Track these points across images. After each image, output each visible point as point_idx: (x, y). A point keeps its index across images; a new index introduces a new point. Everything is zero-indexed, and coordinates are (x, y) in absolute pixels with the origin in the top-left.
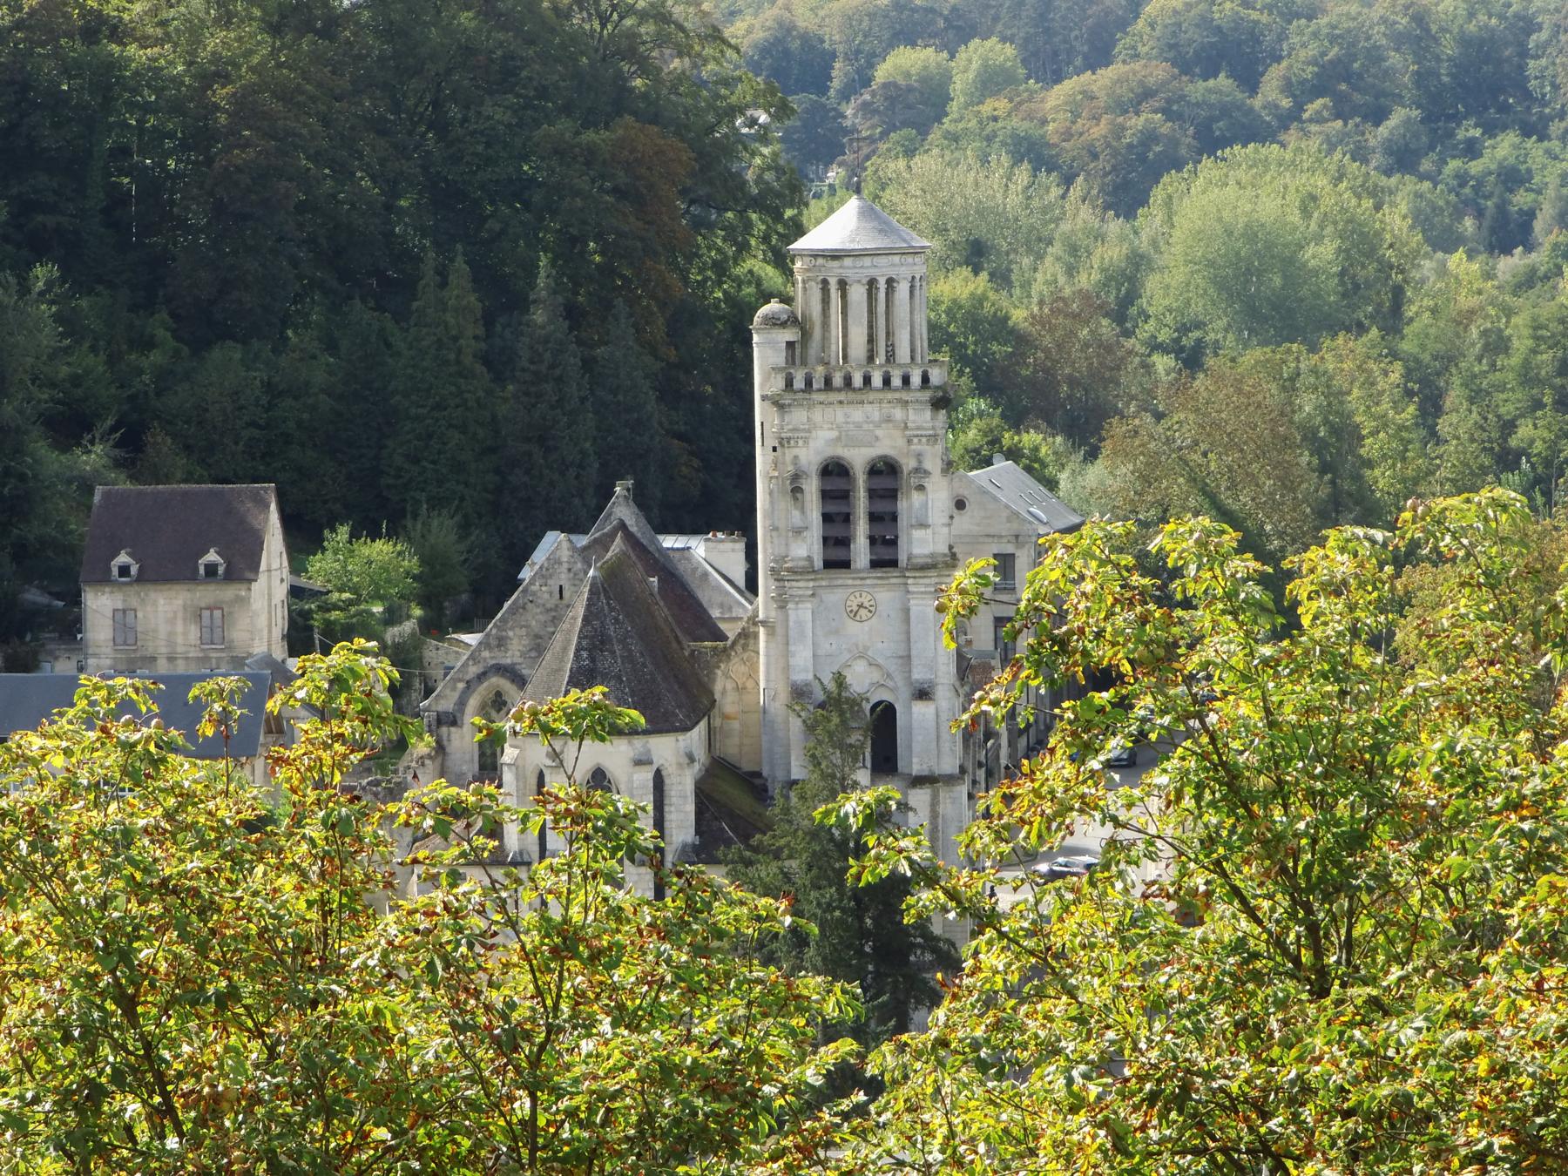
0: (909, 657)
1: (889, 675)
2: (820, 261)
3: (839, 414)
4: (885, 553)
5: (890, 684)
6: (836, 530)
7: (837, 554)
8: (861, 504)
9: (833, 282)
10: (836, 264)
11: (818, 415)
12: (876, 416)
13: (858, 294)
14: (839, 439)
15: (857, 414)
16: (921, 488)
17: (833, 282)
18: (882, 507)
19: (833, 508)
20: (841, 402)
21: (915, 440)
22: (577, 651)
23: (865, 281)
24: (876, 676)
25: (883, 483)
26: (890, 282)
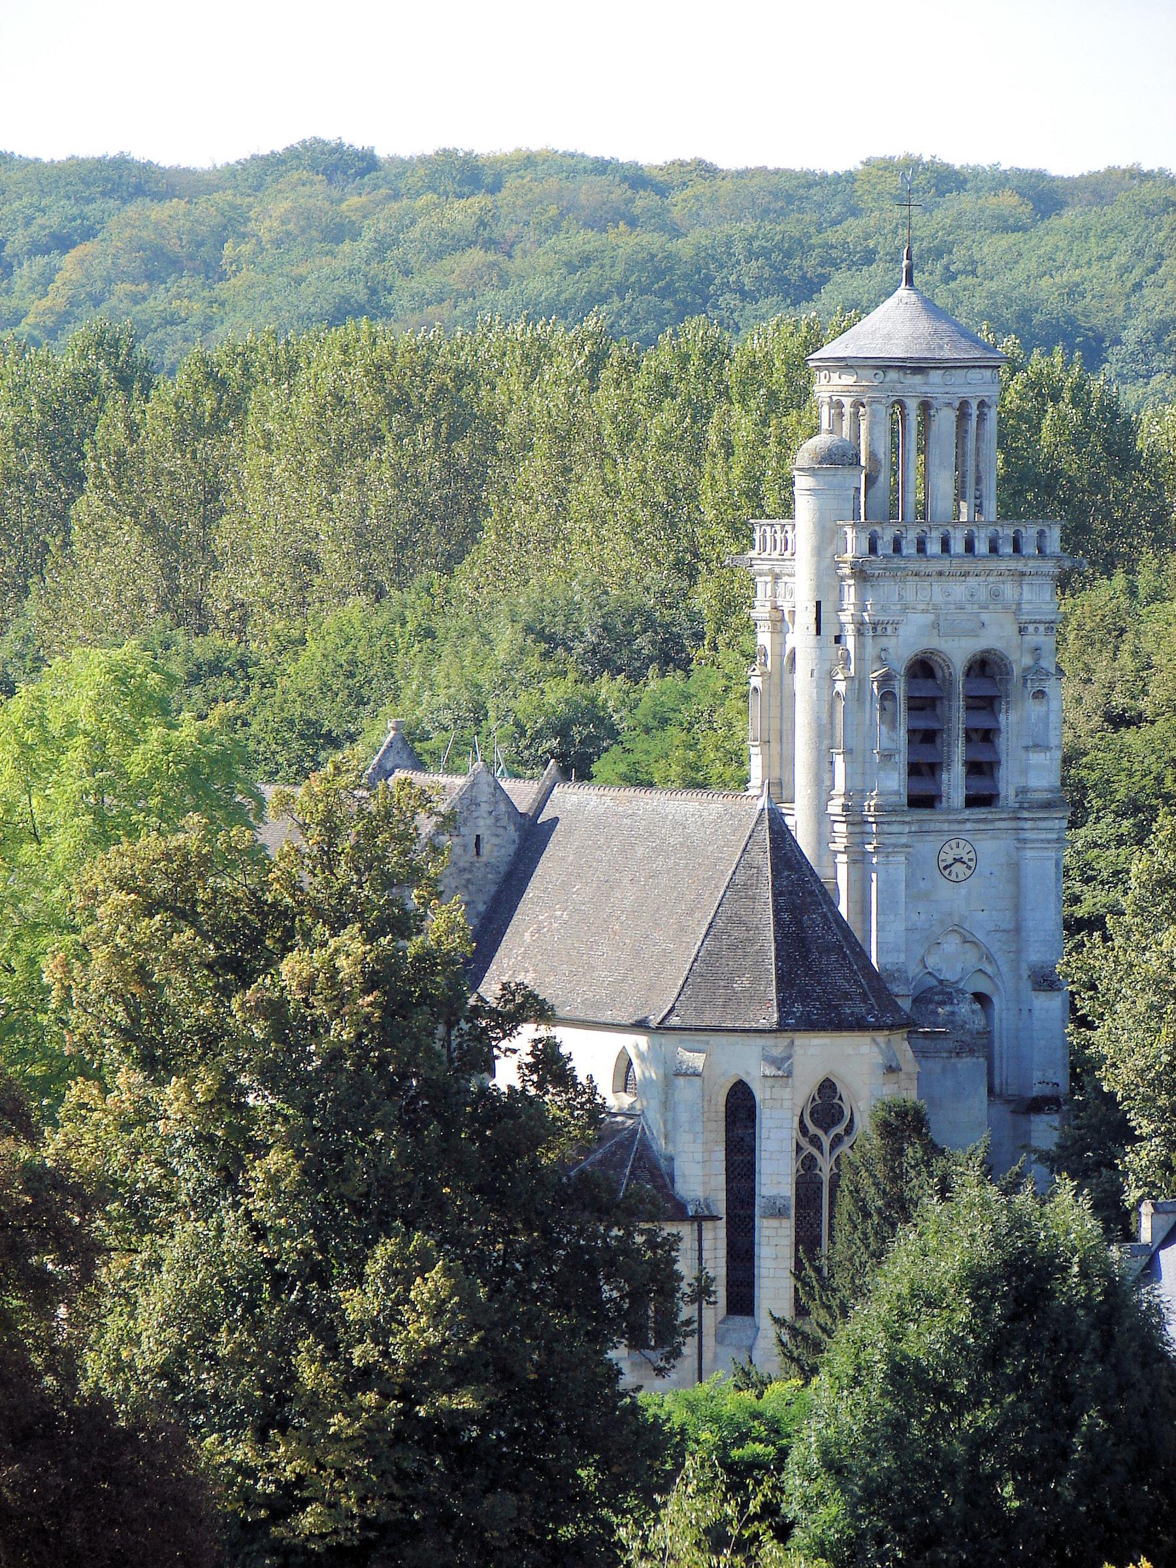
0: (1018, 930)
1: (990, 958)
2: (893, 375)
3: (937, 591)
4: (982, 786)
5: (989, 969)
6: (926, 755)
7: (924, 787)
8: (958, 718)
9: (912, 405)
10: (918, 379)
11: (912, 591)
12: (983, 595)
13: (944, 420)
14: (936, 625)
15: (959, 590)
16: (1040, 694)
17: (912, 405)
18: (982, 721)
19: (922, 724)
20: (940, 574)
21: (1031, 628)
22: (777, 912)
23: (957, 404)
24: (971, 958)
25: (986, 689)
26: (982, 404)
